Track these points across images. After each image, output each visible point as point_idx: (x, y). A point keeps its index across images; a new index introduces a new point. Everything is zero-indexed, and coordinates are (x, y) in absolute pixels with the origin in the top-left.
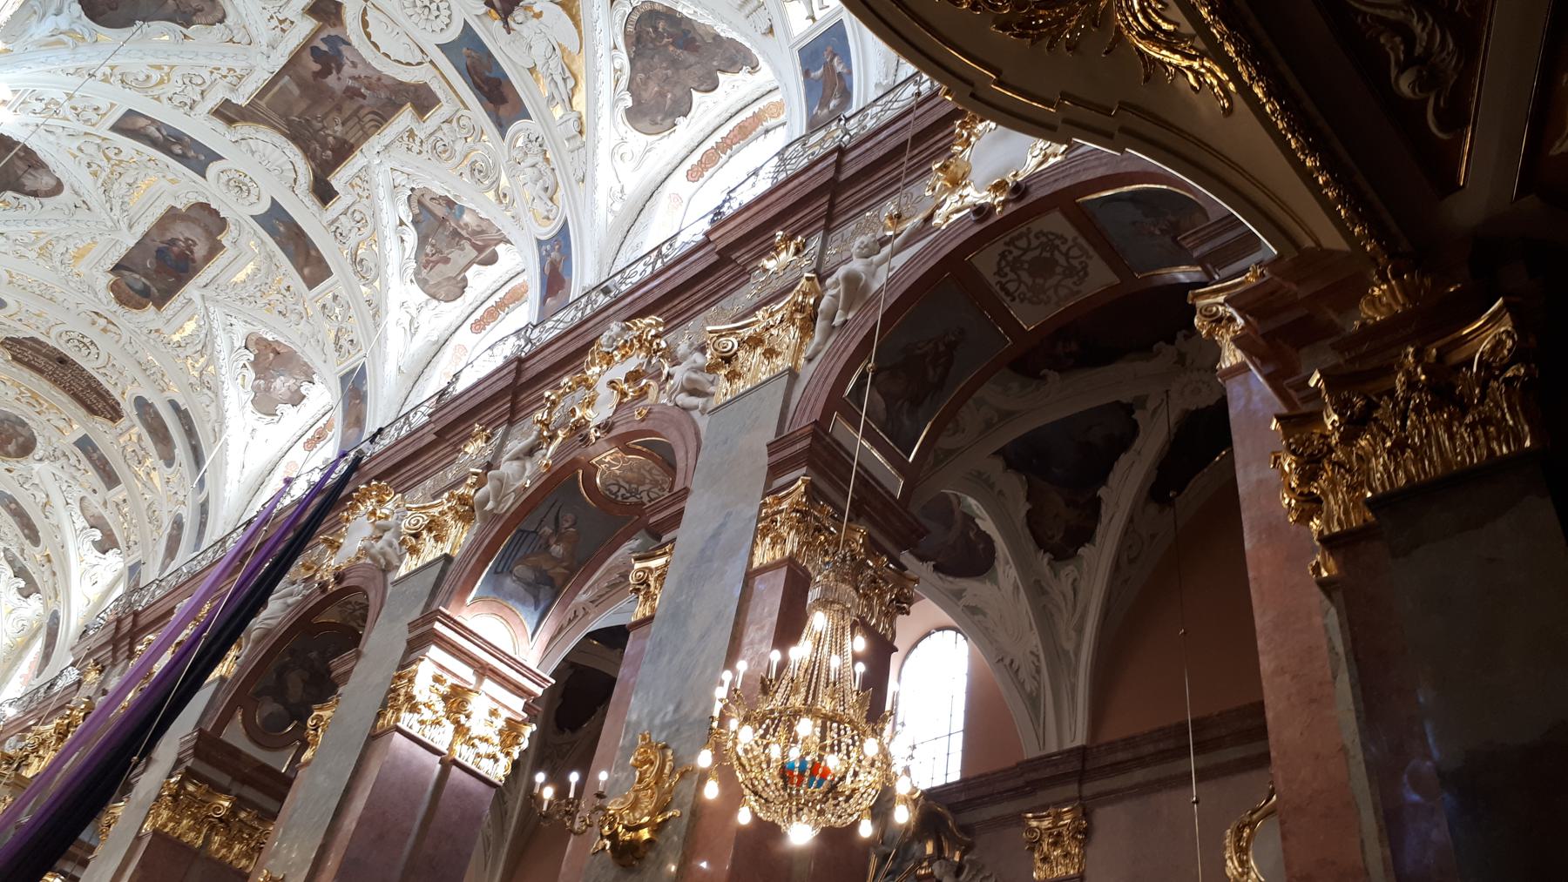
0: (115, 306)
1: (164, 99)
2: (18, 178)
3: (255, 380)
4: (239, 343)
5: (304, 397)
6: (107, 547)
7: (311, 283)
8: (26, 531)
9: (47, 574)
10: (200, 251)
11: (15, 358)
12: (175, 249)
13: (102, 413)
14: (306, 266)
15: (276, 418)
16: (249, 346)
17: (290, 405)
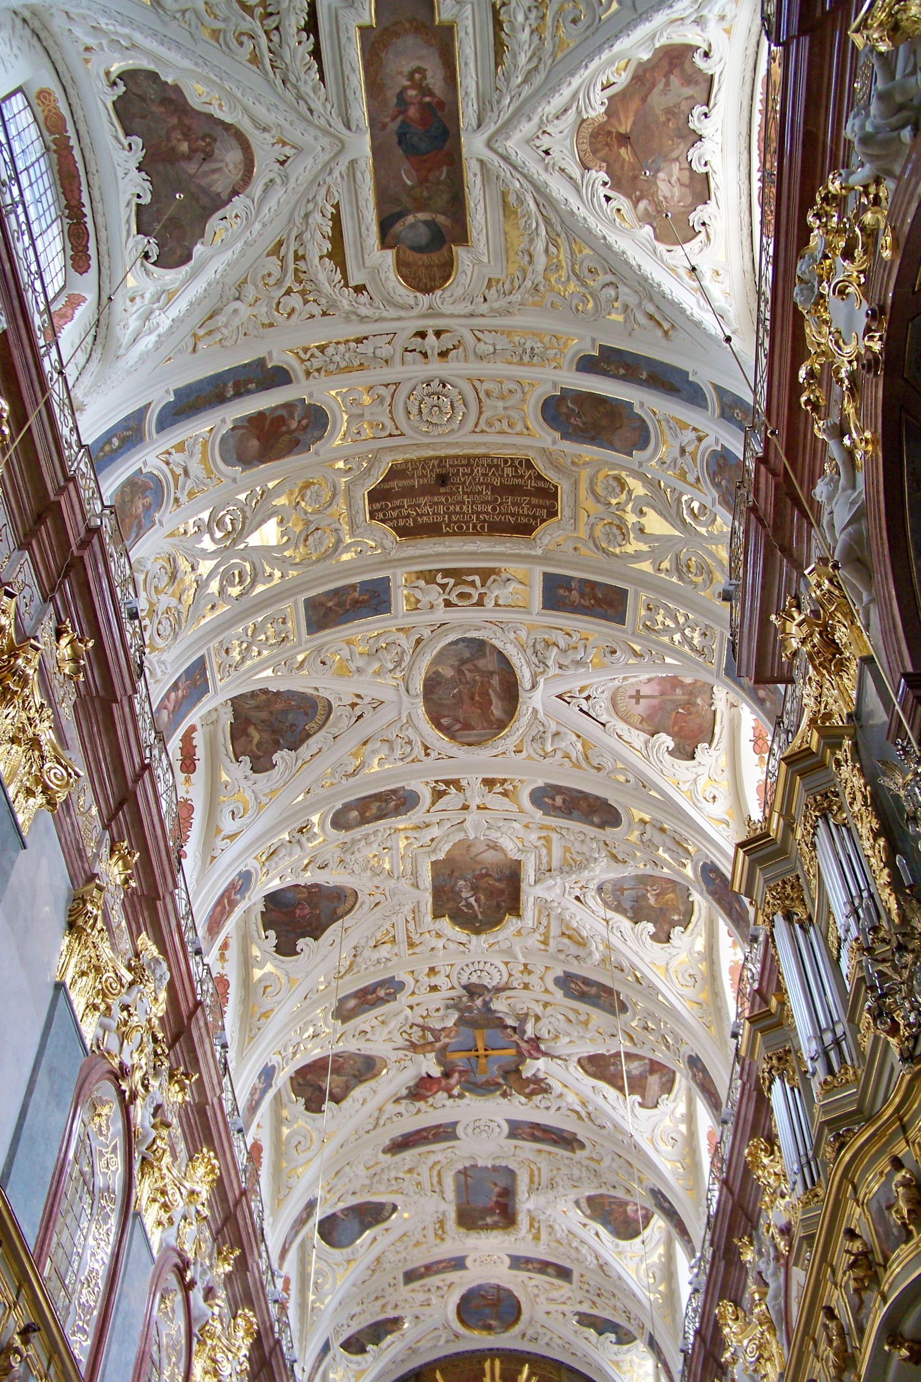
0: (425, 300)
2: (206, 191)
3: (635, 205)
4: (575, 171)
5: (707, 174)
6: (689, 749)
8: (596, 820)
10: (435, 79)
11: (402, 532)
13: (535, 517)
15: (702, 236)
16: (591, 165)
17: (700, 207)
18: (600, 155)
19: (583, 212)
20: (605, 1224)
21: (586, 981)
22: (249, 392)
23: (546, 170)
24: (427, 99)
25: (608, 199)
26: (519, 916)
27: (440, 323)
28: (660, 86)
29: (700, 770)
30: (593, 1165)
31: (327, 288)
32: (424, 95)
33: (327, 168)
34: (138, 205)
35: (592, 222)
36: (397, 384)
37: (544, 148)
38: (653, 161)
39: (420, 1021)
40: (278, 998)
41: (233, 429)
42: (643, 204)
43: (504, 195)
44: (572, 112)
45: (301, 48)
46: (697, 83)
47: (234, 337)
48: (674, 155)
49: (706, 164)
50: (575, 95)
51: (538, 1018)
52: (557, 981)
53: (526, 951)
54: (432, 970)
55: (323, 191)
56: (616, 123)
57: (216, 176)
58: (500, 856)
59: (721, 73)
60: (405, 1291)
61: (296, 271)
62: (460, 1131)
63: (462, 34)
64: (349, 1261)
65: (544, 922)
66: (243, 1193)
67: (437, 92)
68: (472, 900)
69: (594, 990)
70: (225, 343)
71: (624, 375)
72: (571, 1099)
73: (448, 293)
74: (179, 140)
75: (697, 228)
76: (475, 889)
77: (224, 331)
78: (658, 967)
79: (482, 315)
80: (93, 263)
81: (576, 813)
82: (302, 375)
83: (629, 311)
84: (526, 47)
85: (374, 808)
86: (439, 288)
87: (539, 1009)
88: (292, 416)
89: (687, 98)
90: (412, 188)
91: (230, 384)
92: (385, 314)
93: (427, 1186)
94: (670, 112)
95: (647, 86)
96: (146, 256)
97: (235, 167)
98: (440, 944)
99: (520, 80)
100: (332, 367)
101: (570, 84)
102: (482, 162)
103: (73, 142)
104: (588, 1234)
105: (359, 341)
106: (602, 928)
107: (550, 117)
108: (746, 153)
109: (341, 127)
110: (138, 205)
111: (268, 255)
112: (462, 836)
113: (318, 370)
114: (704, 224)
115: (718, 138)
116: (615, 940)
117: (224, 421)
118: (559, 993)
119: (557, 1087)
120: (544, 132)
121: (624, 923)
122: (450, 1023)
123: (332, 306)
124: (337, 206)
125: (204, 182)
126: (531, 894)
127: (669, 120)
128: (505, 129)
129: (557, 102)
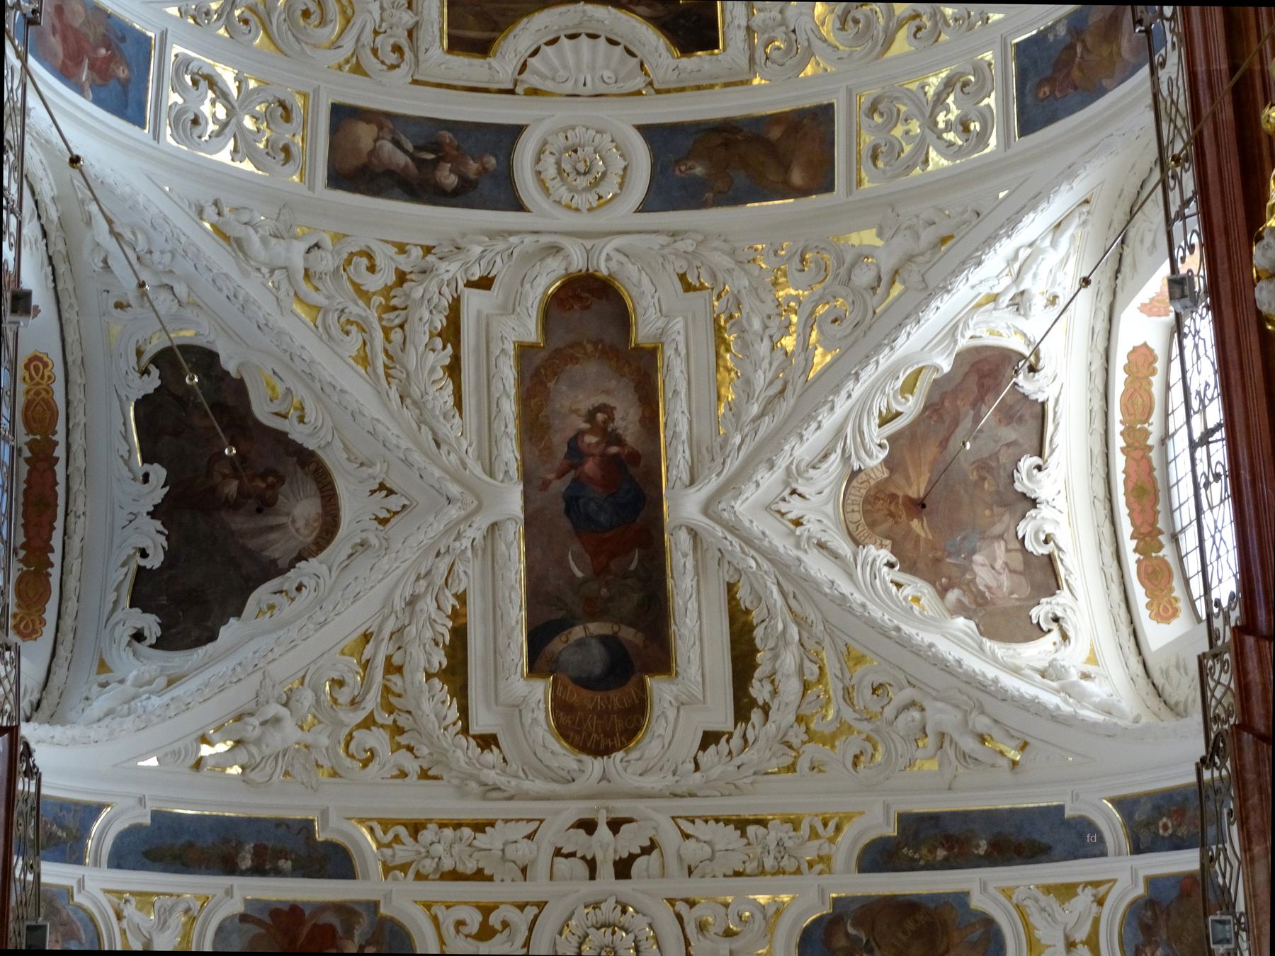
0: (595, 765)
1: (369, 61)
3: (942, 592)
4: (845, 548)
5: (1050, 557)
7: (822, 181)
10: (626, 420)
12: (590, 467)
14: (787, 169)
18: (880, 528)
19: (858, 598)
22: (278, 873)
23: (798, 546)
24: (614, 450)
25: (899, 585)
27: (622, 808)
28: (966, 423)
31: (431, 723)
32: (609, 444)
33: (455, 531)
34: (141, 569)
35: (876, 612)
36: (541, 905)
37: (792, 516)
38: (964, 539)
41: (244, 918)
42: (953, 595)
43: (731, 588)
44: (835, 458)
45: (431, 356)
46: (1021, 420)
47: (268, 770)
48: (998, 529)
49: (1046, 542)
50: (839, 432)
55: (443, 566)
56: (903, 482)
57: (273, 536)
59: (1057, 401)
61: (386, 690)
63: (669, 352)
67: (630, 439)
70: (252, 775)
71: (946, 859)
73: (634, 755)
74: (225, 476)
75: (1045, 628)
77: (254, 749)
79: (691, 795)
80: (49, 631)
82: (376, 869)
83: (946, 744)
84: (765, 364)
86: (619, 750)
88: (349, 933)
89: (1009, 445)
90: (585, 581)
91: (249, 847)
92: (527, 785)
94: (985, 466)
95: (948, 419)
96: (138, 636)
97: (307, 525)
99: (755, 409)
100: (428, 866)
101: (832, 409)
102: (694, 534)
103: (60, 452)
105: (479, 827)
107: (803, 465)
108: (1107, 524)
109: (478, 471)
110: (141, 569)
111: (342, 653)
113: (404, 868)
114: (1056, 620)
115: (1060, 502)
117: (229, 892)
120: (794, 492)
123: (437, 763)
124: (462, 598)
125: (252, 544)
127: (983, 479)
128: (732, 486)
129: (814, 439)
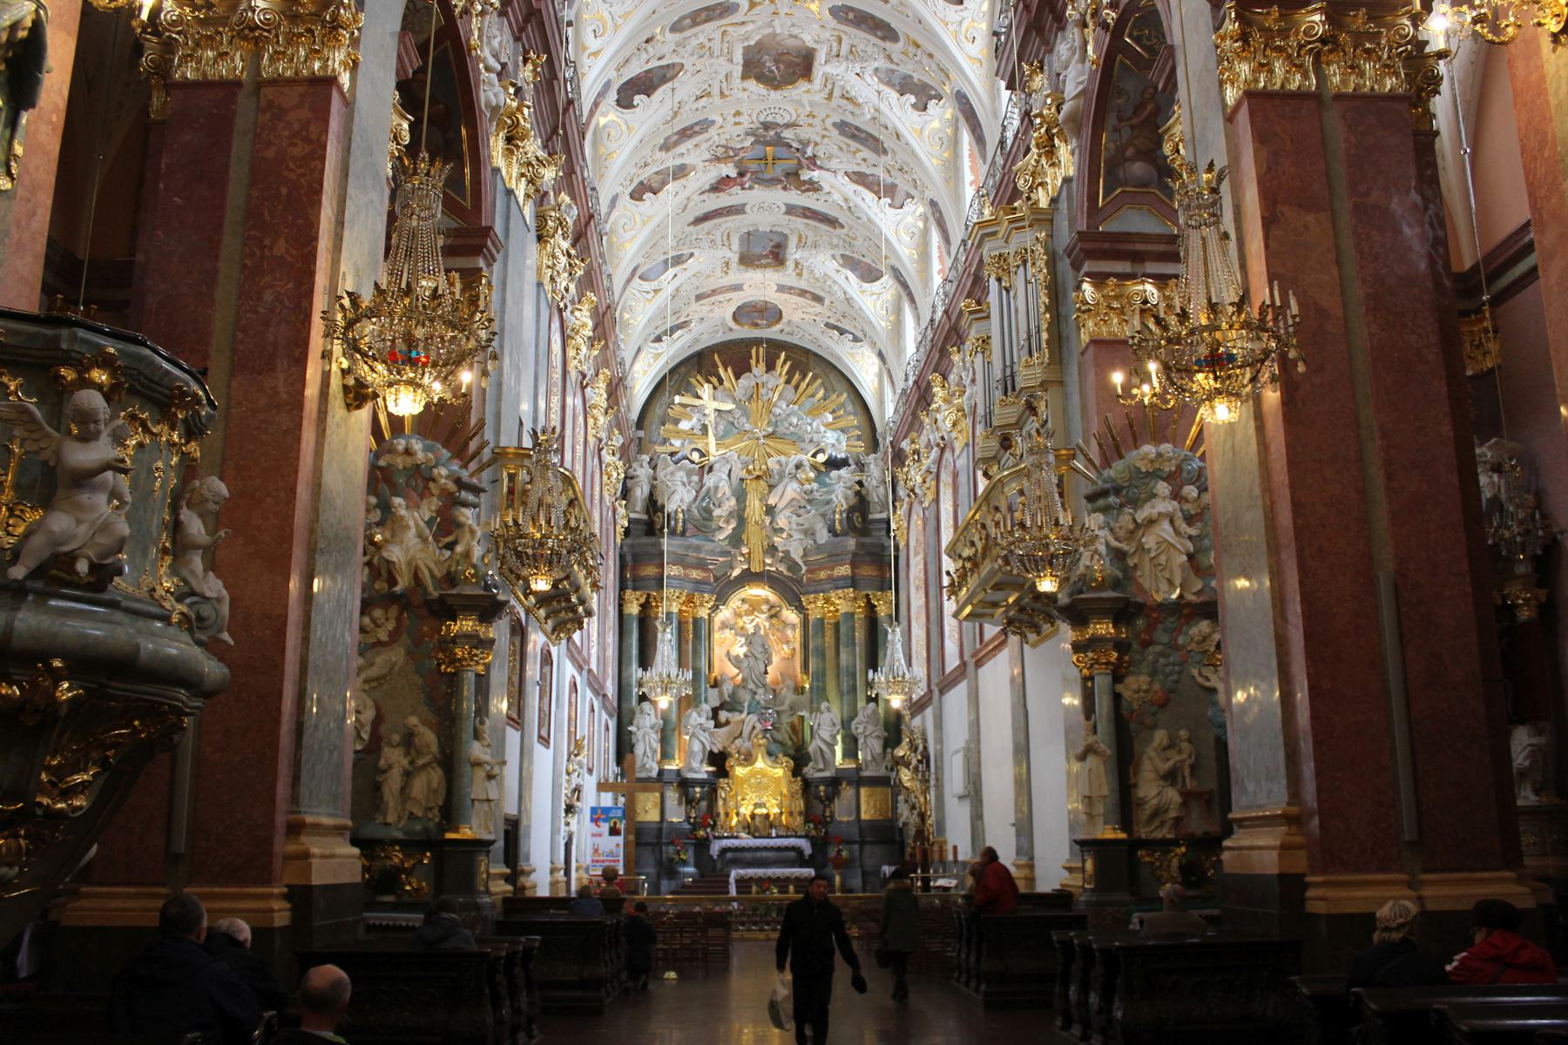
8: (879, 33)
9: (925, 60)
20: (852, 270)
21: (857, 128)
26: (810, 81)
29: (965, 14)
30: (848, 239)
39: (723, 142)
40: (620, 142)
51: (816, 144)
52: (835, 125)
53: (812, 104)
54: (738, 114)
58: (799, 43)
60: (695, 306)
62: (747, 209)
64: (656, 291)
65: (829, 87)
66: (608, 307)
68: (774, 68)
69: (863, 135)
72: (836, 197)
76: (776, 61)
78: (915, 131)
81: (864, 26)
85: (703, 16)
87: (818, 139)
93: (719, 242)
98: (745, 95)
104: (840, 279)
106: (874, 98)
112: (771, 30)
116: (884, 107)
118: (835, 133)
119: (826, 188)
121: (894, 95)
122: (747, 144)
126: (820, 69)
